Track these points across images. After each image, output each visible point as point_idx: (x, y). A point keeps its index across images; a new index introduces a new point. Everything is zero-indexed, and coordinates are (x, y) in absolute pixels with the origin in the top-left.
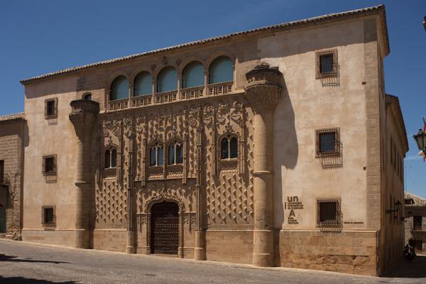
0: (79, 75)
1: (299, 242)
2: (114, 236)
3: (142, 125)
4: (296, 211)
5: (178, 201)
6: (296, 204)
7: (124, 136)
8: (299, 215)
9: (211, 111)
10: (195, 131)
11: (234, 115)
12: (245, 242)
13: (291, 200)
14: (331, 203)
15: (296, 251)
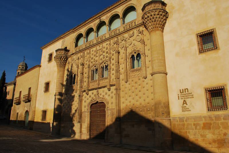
1: (194, 127)
3: (88, 56)
4: (188, 101)
6: (185, 94)
7: (80, 65)
8: (191, 104)
11: (138, 37)
13: (183, 92)
14: (219, 90)
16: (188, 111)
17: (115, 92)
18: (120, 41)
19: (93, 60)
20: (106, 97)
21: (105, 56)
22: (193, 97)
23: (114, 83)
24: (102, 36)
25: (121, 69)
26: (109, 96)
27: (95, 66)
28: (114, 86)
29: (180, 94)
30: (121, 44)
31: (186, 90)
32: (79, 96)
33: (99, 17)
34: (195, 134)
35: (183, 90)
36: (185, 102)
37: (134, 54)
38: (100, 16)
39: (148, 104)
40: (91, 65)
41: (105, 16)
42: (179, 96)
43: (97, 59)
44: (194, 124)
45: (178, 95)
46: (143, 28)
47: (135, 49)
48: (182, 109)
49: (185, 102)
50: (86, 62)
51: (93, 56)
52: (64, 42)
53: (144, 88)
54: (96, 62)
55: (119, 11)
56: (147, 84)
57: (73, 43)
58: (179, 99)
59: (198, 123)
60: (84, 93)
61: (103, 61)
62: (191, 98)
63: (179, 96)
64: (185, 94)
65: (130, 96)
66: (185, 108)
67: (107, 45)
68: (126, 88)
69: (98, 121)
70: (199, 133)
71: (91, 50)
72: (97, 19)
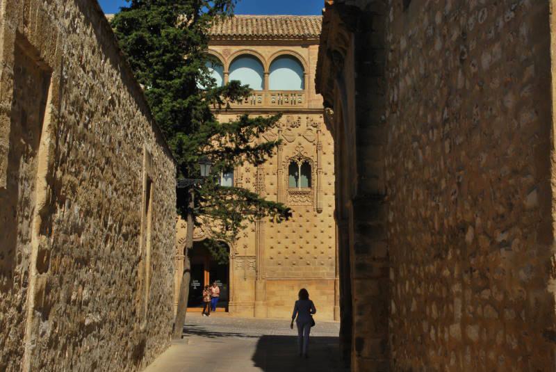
11: (309, 132)
12: (323, 294)
41: (222, 48)
46: (321, 117)
47: (302, 153)
53: (315, 226)
55: (264, 55)
56: (322, 221)
65: (287, 238)
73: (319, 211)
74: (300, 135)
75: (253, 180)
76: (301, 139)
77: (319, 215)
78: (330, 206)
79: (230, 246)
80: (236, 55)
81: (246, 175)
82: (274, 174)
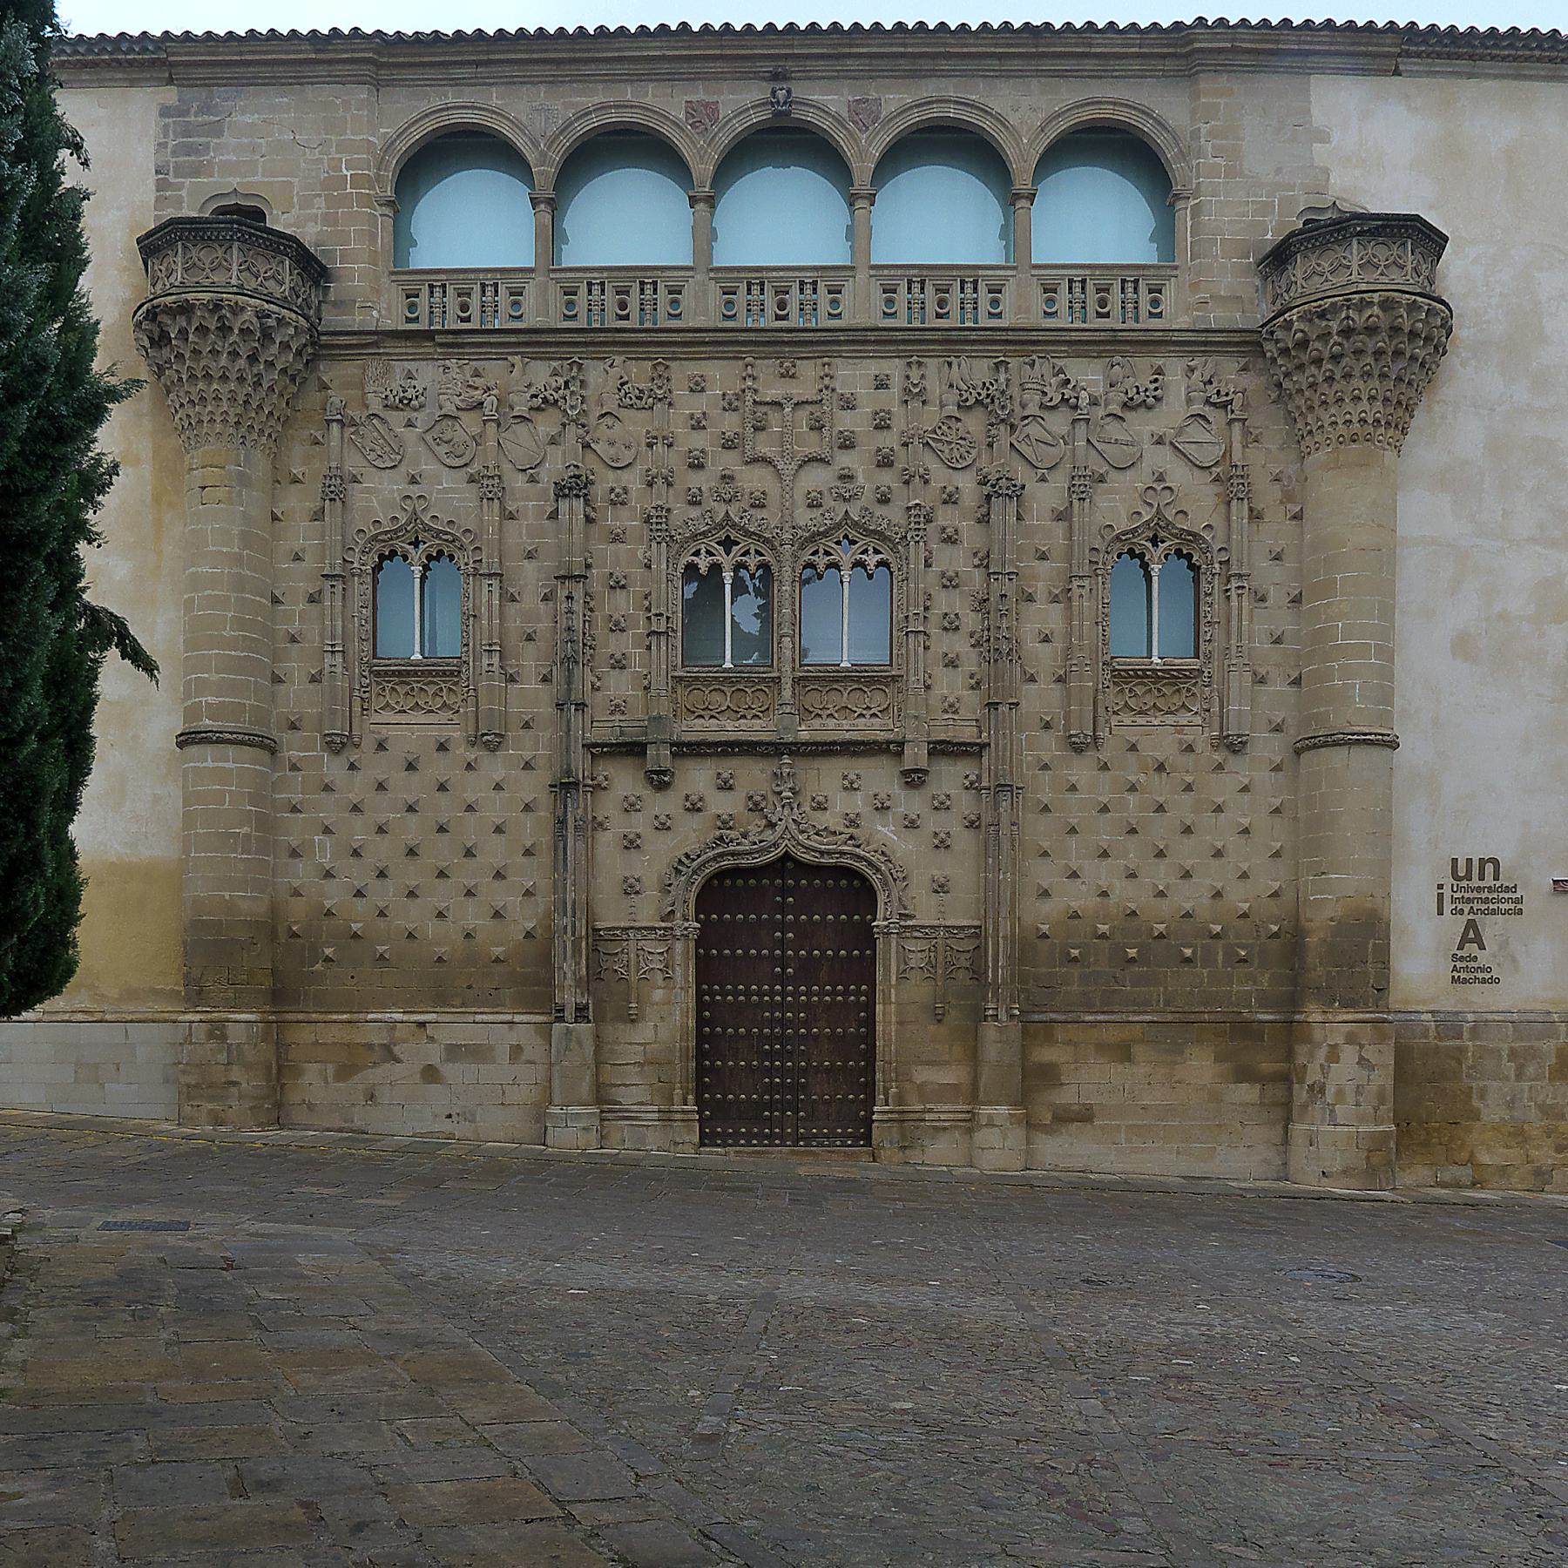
0: (170, 81)
1: (1509, 1068)
2: (454, 1052)
3: (636, 425)
4: (1491, 928)
5: (876, 859)
6: (1478, 889)
8: (1503, 946)
9: (1064, 401)
10: (966, 484)
11: (1196, 432)
12: (1244, 1074)
13: (1469, 877)
15: (1492, 1112)
16: (1484, 981)
17: (965, 804)
18: (1032, 409)
19: (698, 480)
20: (885, 831)
21: (861, 480)
22: (1520, 912)
23: (967, 734)
24: (808, 276)
25: (1028, 630)
26: (912, 825)
27: (728, 544)
28: (966, 754)
29: (1449, 881)
30: (1034, 430)
31: (1489, 868)
32: (565, 787)
33: (768, 67)
34: (1513, 1101)
35: (1469, 861)
36: (1471, 935)
37: (1149, 545)
38: (790, 65)
39: (1242, 921)
40: (681, 512)
42: (1440, 897)
43: (754, 480)
44: (1513, 1054)
45: (1440, 887)
47: (1169, 514)
48: (1455, 969)
49: (1471, 935)
50: (605, 482)
51: (699, 441)
52: (216, 130)
53: (1219, 809)
54: (759, 514)
55: (1013, 119)
56: (1245, 789)
57: (365, 201)
58: (1440, 913)
59: (1532, 1047)
60: (624, 780)
61: (838, 526)
62: (1507, 912)
63: (1440, 897)
64: (1479, 889)
65: (1105, 854)
66: (1472, 964)
67: (881, 384)
68: (1073, 788)
69: (782, 1007)
70: (1531, 1099)
71: (681, 372)
72: (757, 76)
73: (1235, 746)
74: (1160, 442)
75: (970, 621)
76: (1161, 458)
77: (1233, 762)
78: (1278, 729)
79: (877, 885)
80: (901, 124)
81: (944, 602)
82: (1055, 600)
